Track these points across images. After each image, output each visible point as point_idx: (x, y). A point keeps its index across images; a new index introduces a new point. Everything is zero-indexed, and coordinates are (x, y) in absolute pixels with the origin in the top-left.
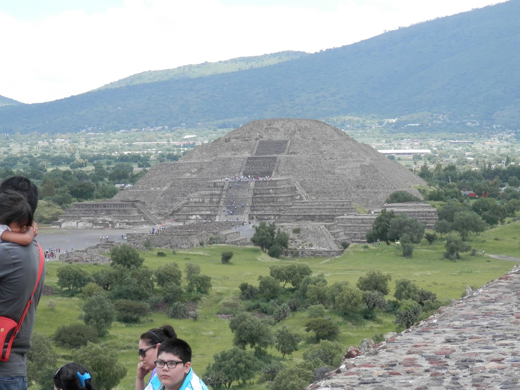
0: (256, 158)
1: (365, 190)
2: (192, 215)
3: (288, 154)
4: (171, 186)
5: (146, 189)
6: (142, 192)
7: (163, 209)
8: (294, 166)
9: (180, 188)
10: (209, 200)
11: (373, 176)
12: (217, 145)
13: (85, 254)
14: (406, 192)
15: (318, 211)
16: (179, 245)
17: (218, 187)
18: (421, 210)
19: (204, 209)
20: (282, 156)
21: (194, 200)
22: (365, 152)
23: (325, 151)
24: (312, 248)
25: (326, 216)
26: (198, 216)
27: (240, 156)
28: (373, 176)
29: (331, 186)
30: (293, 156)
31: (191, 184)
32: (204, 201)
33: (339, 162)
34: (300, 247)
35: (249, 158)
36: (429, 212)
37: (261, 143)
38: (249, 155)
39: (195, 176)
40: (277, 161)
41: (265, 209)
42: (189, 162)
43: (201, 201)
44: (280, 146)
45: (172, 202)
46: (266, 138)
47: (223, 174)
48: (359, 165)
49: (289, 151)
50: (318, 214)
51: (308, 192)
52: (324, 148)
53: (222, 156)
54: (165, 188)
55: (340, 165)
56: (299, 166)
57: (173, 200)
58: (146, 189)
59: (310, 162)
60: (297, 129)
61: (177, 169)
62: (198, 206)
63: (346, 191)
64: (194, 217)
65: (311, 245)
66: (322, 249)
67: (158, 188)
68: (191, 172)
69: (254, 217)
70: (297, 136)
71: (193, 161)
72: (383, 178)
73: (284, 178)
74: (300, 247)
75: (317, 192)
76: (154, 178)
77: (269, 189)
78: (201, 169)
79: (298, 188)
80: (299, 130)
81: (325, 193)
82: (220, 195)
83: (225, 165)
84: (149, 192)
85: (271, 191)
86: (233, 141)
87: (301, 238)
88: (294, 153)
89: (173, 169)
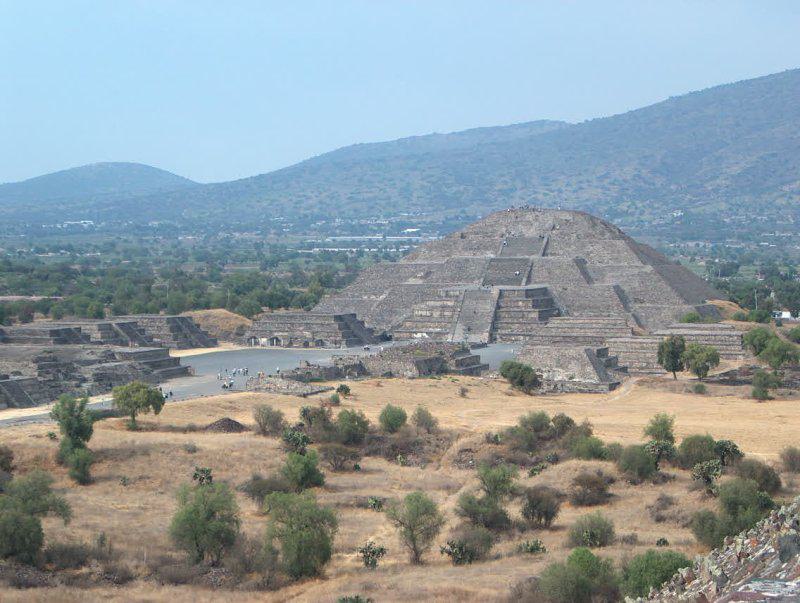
0: (499, 260)
1: (643, 305)
3: (543, 255)
6: (352, 301)
10: (438, 313)
17: (450, 297)
23: (591, 252)
25: (592, 337)
26: (425, 334)
27: (482, 257)
30: (550, 257)
35: (492, 260)
36: (730, 336)
38: (492, 256)
39: (420, 282)
43: (428, 314)
48: (636, 271)
49: (545, 250)
56: (557, 272)
57: (392, 312)
63: (618, 305)
64: (419, 335)
67: (373, 297)
77: (518, 301)
78: (428, 274)
82: (453, 309)
85: (520, 303)
86: (471, 237)
88: (552, 254)
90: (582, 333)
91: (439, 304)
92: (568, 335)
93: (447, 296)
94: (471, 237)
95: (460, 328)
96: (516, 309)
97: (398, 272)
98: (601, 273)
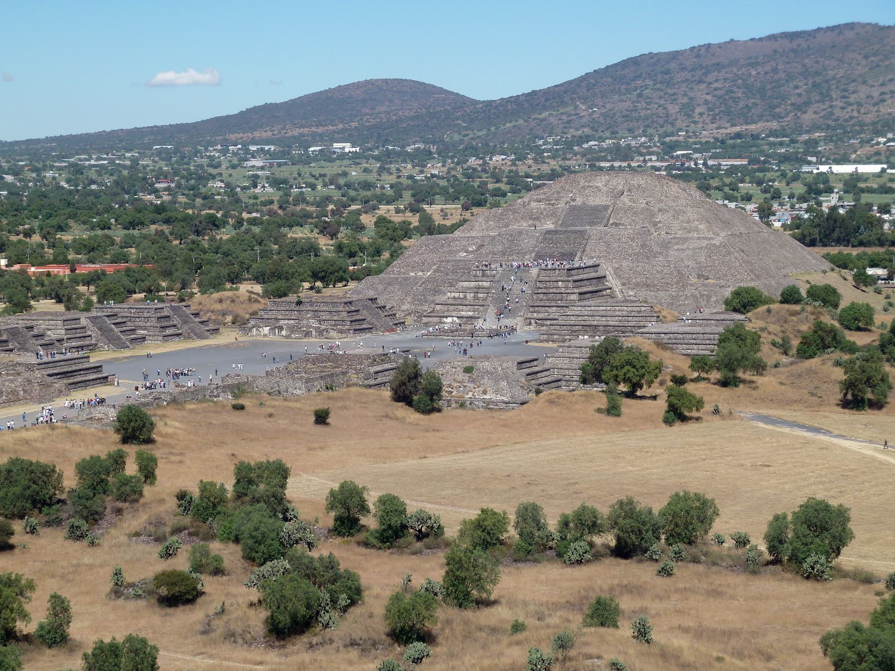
0: (556, 232)
2: (446, 317)
4: (434, 272)
5: (404, 273)
7: (421, 304)
8: (608, 245)
9: (447, 274)
11: (724, 262)
12: (511, 210)
13: (112, 410)
14: (753, 289)
15: (604, 319)
16: (290, 390)
18: (708, 330)
19: (464, 308)
20: (594, 231)
21: (453, 294)
22: (724, 222)
23: (659, 222)
24: (485, 397)
26: (455, 319)
28: (724, 262)
29: (658, 276)
31: (463, 269)
32: (465, 296)
33: (677, 240)
34: (470, 395)
35: (549, 232)
37: (573, 209)
40: (586, 237)
41: (550, 310)
42: (468, 235)
43: (462, 295)
44: (595, 214)
45: (434, 295)
46: (579, 201)
47: (509, 255)
48: (704, 243)
50: (604, 323)
51: (623, 284)
52: (660, 217)
53: (515, 227)
54: (429, 274)
55: (677, 243)
57: (436, 292)
58: (404, 273)
59: (633, 240)
60: (626, 188)
61: (449, 245)
62: (459, 303)
63: (678, 283)
64: (449, 320)
65: (485, 392)
66: (499, 398)
67: (420, 273)
68: (467, 251)
69: (533, 321)
70: (625, 199)
71: (474, 234)
72: (737, 264)
73: (590, 263)
74: (470, 395)
75: (637, 285)
76: (416, 259)
79: (609, 278)
80: (629, 190)
81: (648, 286)
83: (512, 241)
84: (406, 279)
87: (473, 381)
89: (443, 246)
90: (603, 321)
91: (472, 284)
92: (588, 323)
93: (483, 275)
94: (533, 204)
95: (492, 311)
96: (554, 290)
97: (449, 245)
98: (666, 245)
